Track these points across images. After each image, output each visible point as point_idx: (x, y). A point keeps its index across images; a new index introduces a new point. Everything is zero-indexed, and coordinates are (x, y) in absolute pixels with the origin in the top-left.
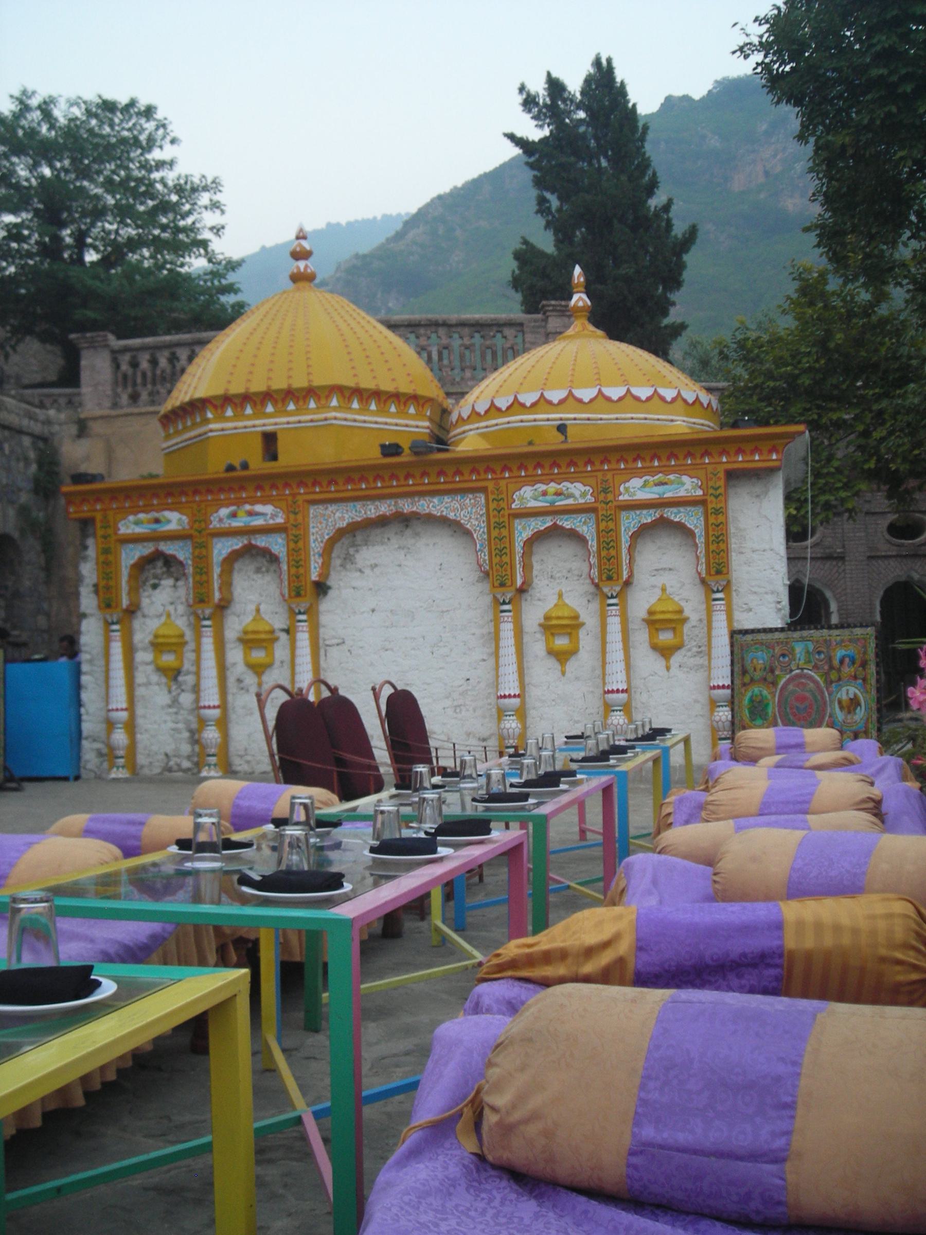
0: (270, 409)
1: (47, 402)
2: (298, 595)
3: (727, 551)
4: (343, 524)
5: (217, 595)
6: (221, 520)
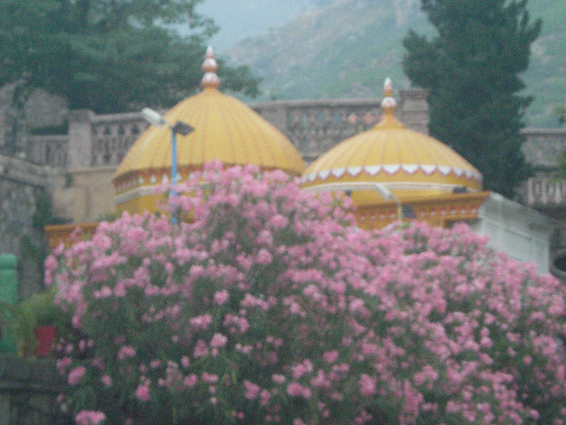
1: (53, 147)
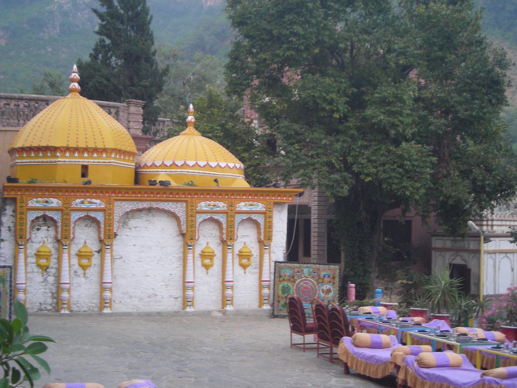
0: (86, 155)
2: (109, 238)
3: (272, 232)
4: (129, 210)
6: (76, 204)
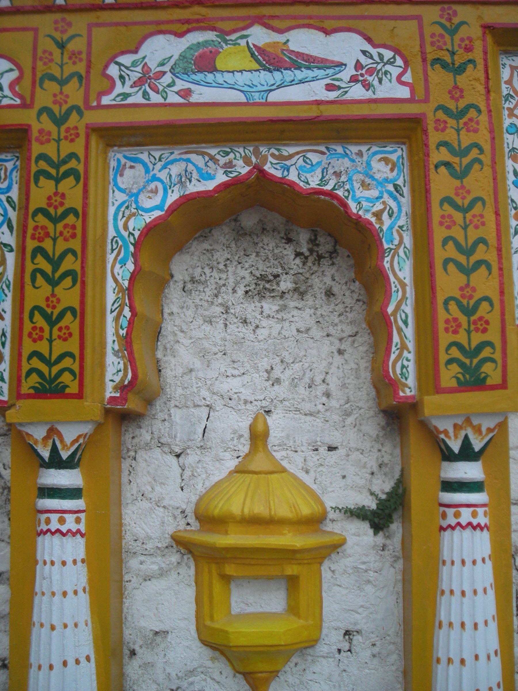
5: (114, 369)
6: (147, 79)
